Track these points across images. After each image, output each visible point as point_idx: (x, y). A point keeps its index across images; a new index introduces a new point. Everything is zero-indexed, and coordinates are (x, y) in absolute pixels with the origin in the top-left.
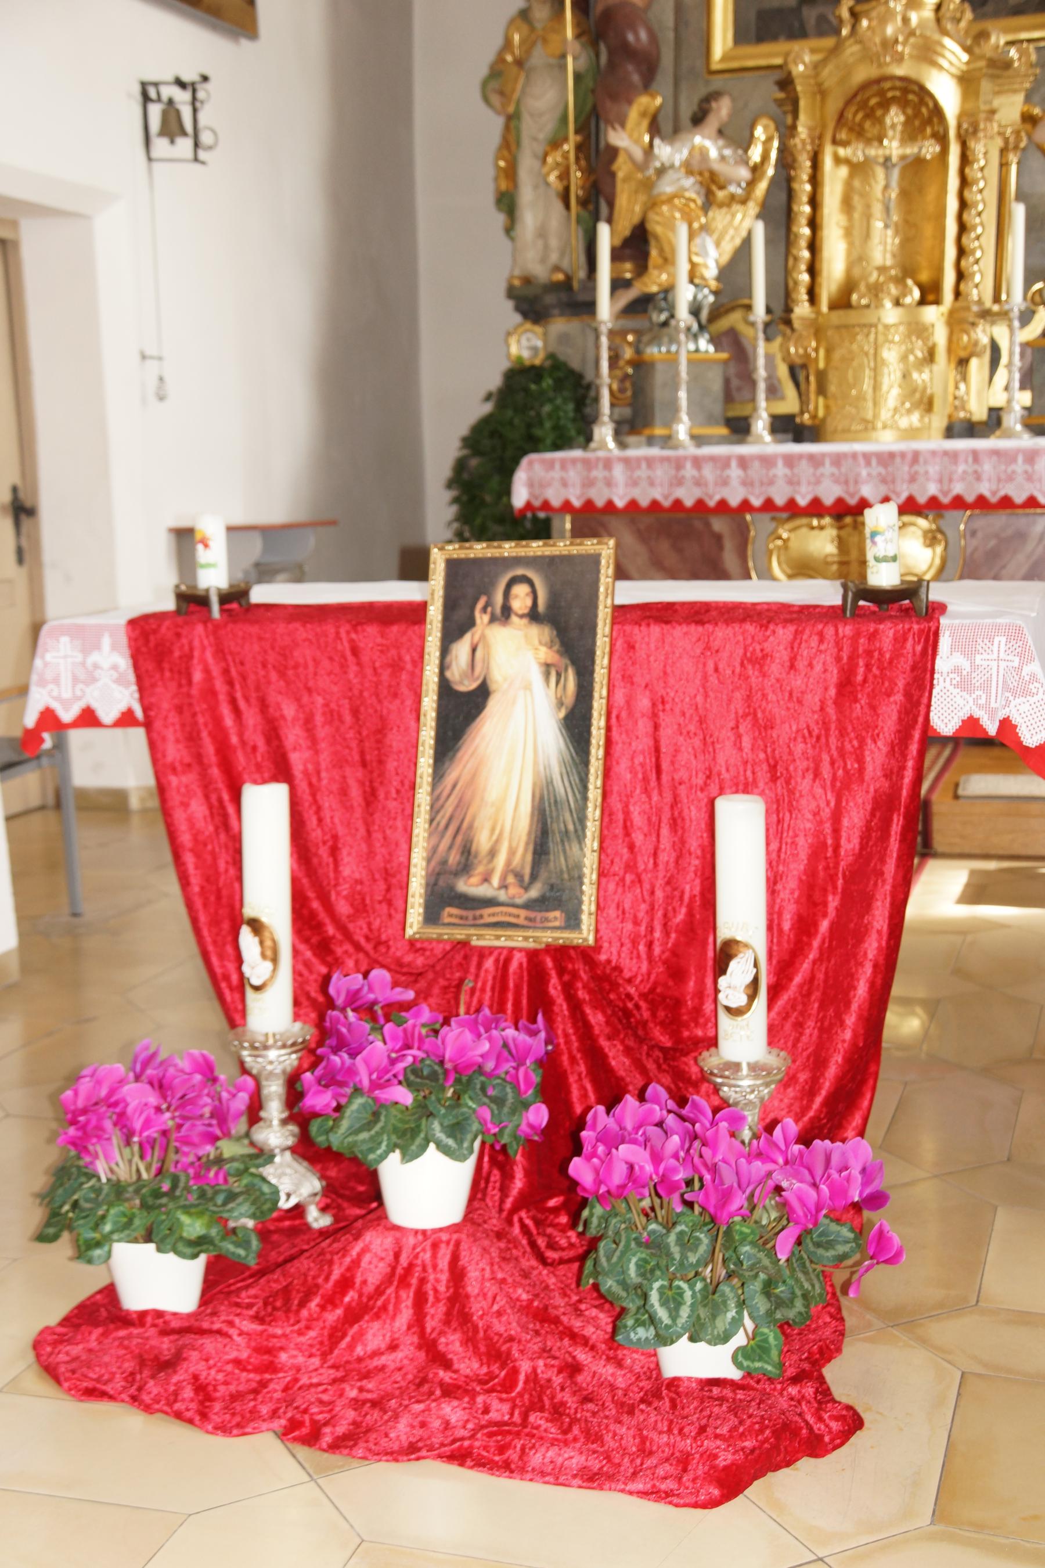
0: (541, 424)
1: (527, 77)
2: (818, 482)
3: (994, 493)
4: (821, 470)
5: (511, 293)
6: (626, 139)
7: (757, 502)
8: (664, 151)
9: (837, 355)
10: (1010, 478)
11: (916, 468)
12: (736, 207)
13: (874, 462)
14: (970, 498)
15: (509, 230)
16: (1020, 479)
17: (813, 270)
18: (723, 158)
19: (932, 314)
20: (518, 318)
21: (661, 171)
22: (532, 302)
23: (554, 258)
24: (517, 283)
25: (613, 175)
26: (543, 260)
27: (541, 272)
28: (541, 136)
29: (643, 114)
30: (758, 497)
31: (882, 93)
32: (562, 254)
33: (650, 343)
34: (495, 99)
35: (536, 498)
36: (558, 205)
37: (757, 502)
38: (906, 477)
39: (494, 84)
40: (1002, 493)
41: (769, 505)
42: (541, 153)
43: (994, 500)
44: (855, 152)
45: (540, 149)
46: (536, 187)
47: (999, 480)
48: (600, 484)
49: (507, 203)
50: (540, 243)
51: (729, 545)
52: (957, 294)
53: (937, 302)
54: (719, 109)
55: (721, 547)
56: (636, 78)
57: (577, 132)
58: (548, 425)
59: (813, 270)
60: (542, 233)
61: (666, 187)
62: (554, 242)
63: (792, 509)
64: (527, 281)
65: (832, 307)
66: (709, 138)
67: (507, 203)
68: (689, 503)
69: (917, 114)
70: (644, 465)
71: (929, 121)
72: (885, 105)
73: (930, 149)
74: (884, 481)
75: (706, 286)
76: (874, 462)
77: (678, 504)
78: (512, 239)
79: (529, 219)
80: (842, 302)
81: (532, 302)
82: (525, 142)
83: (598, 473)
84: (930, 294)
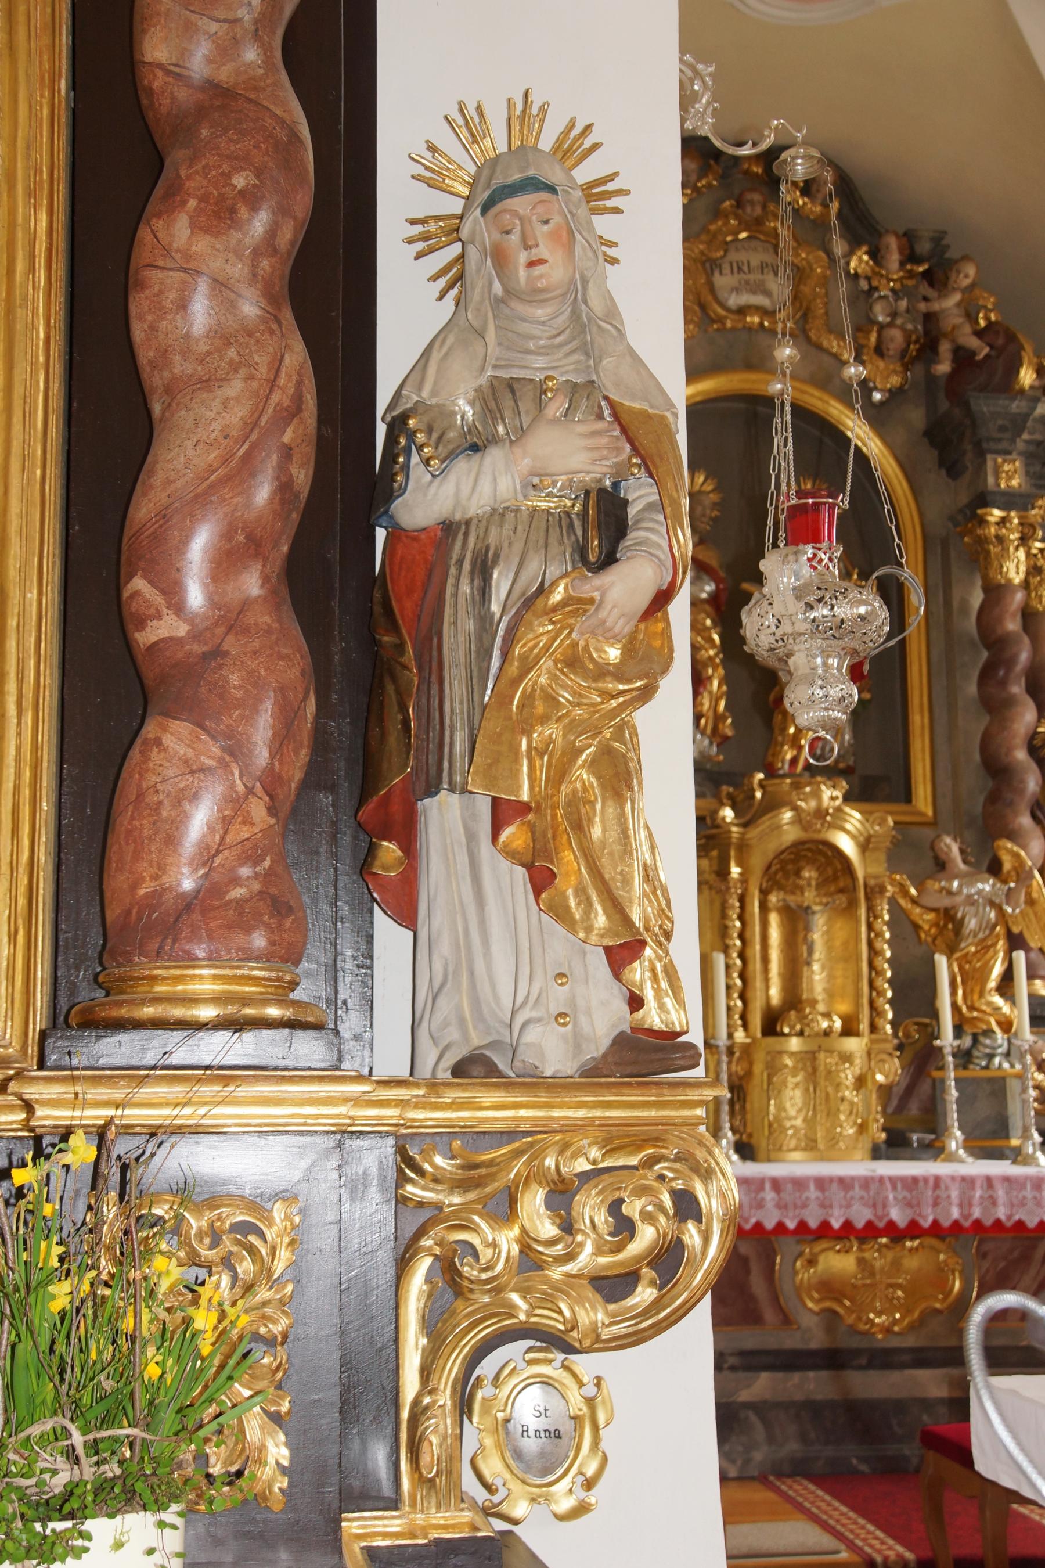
2: (849, 1206)
4: (851, 1193)
7: (791, 1225)
10: (1023, 1204)
11: (938, 1192)
13: (899, 1186)
16: (1030, 1204)
19: (854, 1045)
30: (792, 1219)
37: (791, 1225)
38: (930, 1201)
40: (1017, 1218)
41: (802, 1227)
47: (1012, 1205)
53: (857, 1034)
74: (909, 1205)
76: (899, 1186)
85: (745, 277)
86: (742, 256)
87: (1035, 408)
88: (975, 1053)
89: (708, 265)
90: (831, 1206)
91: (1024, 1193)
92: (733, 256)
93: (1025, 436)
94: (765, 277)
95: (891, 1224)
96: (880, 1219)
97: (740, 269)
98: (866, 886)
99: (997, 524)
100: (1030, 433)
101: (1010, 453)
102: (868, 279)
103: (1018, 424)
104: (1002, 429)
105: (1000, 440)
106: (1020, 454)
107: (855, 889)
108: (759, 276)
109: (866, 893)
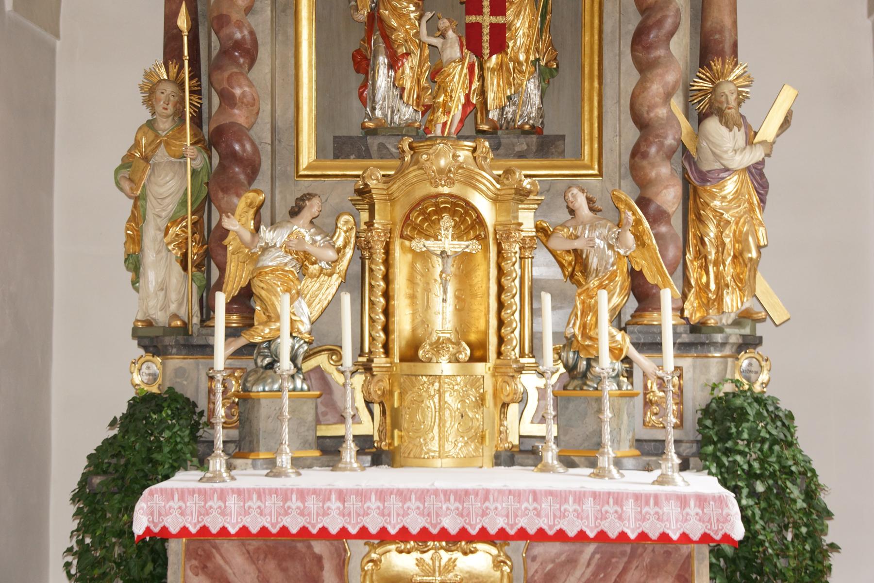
0: (160, 448)
1: (153, 170)
2: (406, 514)
3: (551, 527)
4: (408, 504)
5: (136, 333)
6: (238, 225)
7: (353, 531)
8: (267, 235)
9: (408, 398)
10: (563, 516)
11: (487, 504)
12: (323, 278)
13: (452, 498)
14: (532, 531)
15: (134, 283)
16: (571, 516)
17: (386, 330)
18: (314, 242)
19: (480, 368)
20: (142, 352)
21: (265, 249)
22: (152, 340)
23: (173, 307)
24: (140, 325)
25: (225, 248)
26: (164, 308)
27: (161, 318)
28: (164, 214)
29: (250, 205)
30: (354, 526)
31: (436, 205)
32: (180, 305)
33: (256, 382)
34: (127, 185)
35: (156, 525)
36: (177, 267)
37: (353, 531)
38: (479, 512)
39: (126, 173)
40: (558, 528)
41: (363, 533)
42: (163, 228)
43: (551, 533)
44: (419, 244)
45: (163, 224)
46: (158, 252)
47: (555, 516)
48: (215, 513)
49: (134, 264)
50: (161, 294)
51: (328, 565)
52: (499, 354)
53: (483, 359)
54: (312, 206)
55: (321, 568)
56: (242, 177)
57: (193, 214)
58: (166, 449)
59: (386, 330)
60: (163, 287)
61: (270, 261)
62: (173, 296)
63: (384, 536)
64: (149, 323)
65: (402, 359)
66: (303, 227)
67: (134, 264)
68: (294, 530)
69: (463, 221)
70: (255, 496)
71: (472, 227)
72: (439, 211)
73: (474, 246)
74: (461, 515)
75: (302, 339)
76: (452, 498)
77: (284, 531)
78: (137, 290)
79: (152, 277)
80: (411, 355)
81: (152, 340)
82: (150, 216)
83: (214, 503)
84: (478, 355)
88: (589, 375)
90: (389, 515)
91: (566, 506)
95: (443, 530)
96: (434, 526)
98: (495, 233)
107: (487, 236)
109: (496, 239)
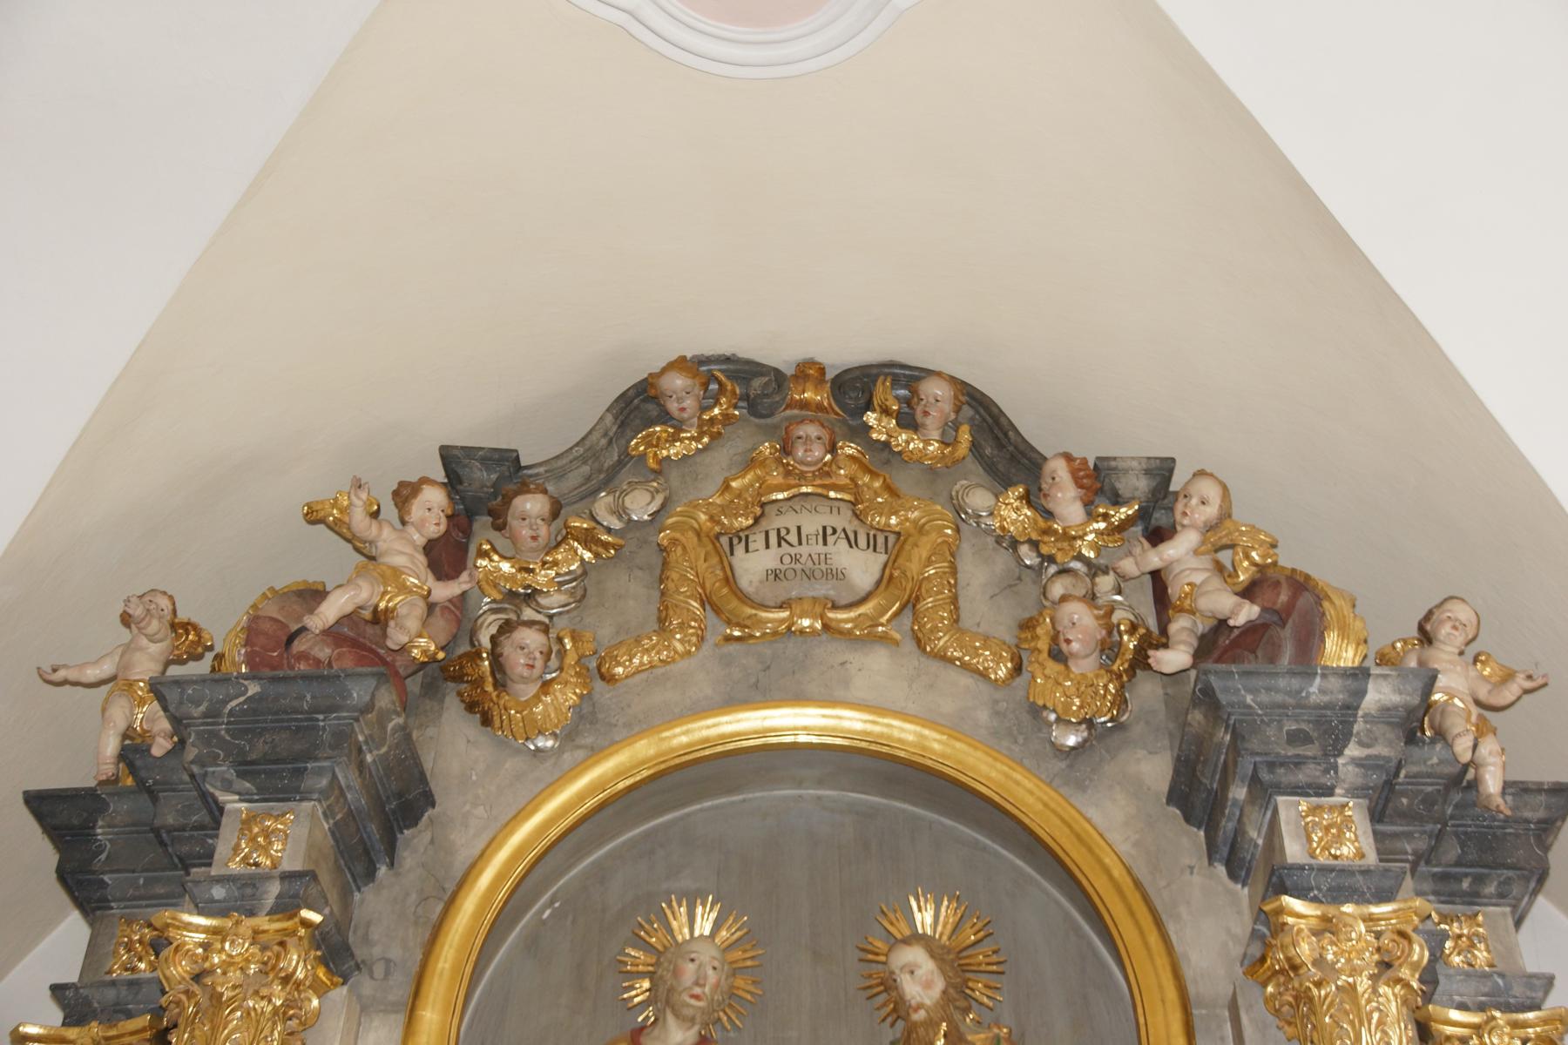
85: (793, 551)
86: (788, 521)
87: (1362, 693)
89: (724, 540)
92: (775, 522)
93: (1353, 750)
94: (830, 548)
97: (780, 538)
99: (1317, 933)
100: (1361, 744)
101: (1329, 792)
102: (1035, 545)
103: (1334, 727)
104: (1295, 738)
105: (1299, 762)
106: (1353, 792)
108: (820, 548)
